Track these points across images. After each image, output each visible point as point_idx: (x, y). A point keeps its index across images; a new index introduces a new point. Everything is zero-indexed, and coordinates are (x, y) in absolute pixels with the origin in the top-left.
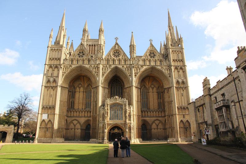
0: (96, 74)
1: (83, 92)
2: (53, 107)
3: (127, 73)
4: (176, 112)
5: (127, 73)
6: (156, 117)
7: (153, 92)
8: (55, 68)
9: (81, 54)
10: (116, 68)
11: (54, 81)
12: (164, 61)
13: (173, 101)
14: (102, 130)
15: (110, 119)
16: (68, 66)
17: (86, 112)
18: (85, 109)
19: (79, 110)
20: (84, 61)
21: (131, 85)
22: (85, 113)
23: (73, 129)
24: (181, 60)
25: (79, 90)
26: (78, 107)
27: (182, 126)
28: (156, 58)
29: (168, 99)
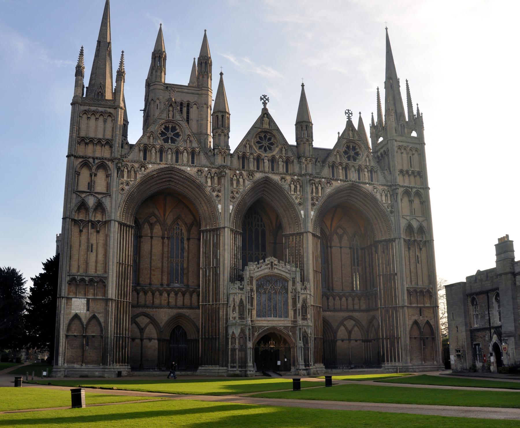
0: (215, 194)
1: (163, 238)
2: (101, 280)
3: (294, 197)
4: (403, 300)
5: (295, 197)
6: (347, 310)
7: (341, 248)
8: (98, 168)
9: (170, 134)
10: (266, 181)
11: (100, 206)
12: (379, 173)
13: (399, 274)
14: (239, 343)
15: (258, 315)
16: (136, 165)
17: (172, 295)
18: (168, 285)
19: (154, 289)
20: (180, 156)
21: (303, 231)
22: (169, 295)
23: (136, 340)
24: (419, 173)
25: (152, 233)
26: (150, 278)
27: (416, 333)
28: (360, 163)
29: (386, 268)
